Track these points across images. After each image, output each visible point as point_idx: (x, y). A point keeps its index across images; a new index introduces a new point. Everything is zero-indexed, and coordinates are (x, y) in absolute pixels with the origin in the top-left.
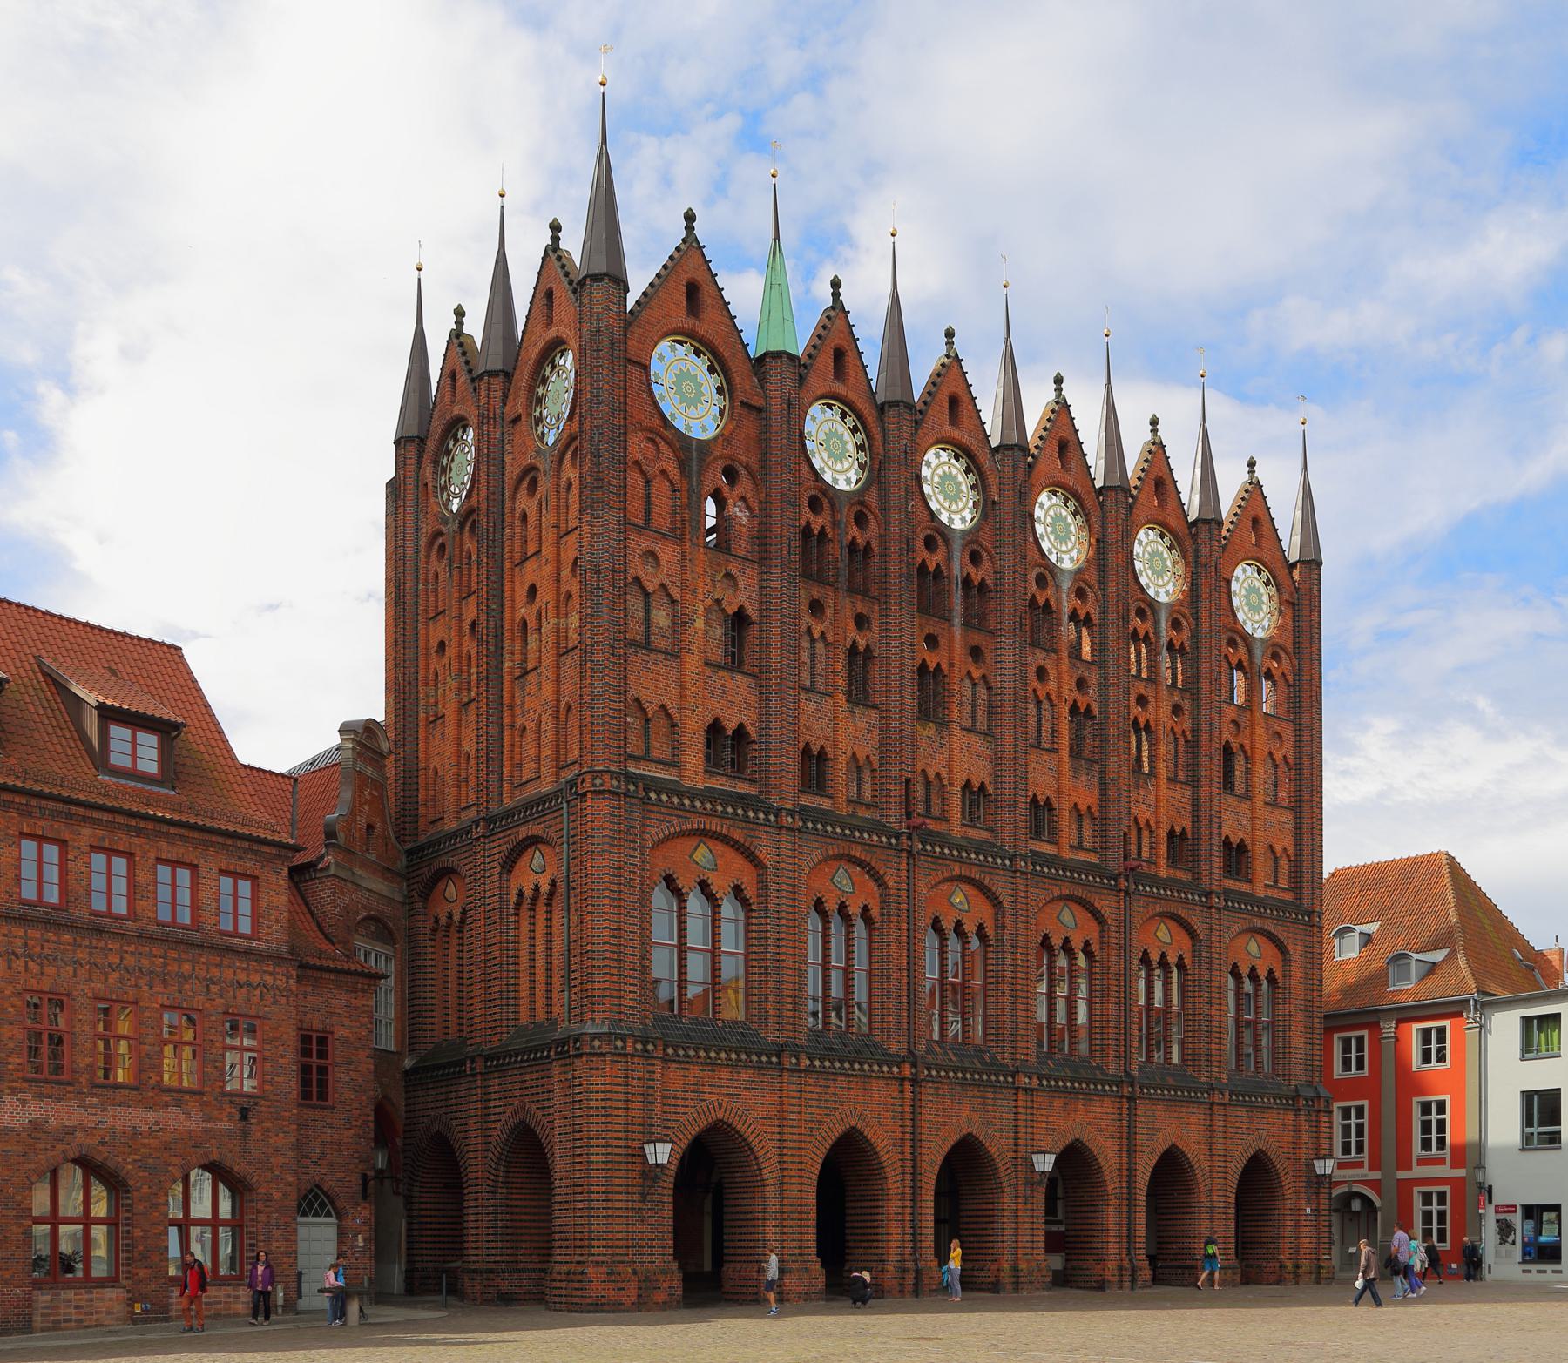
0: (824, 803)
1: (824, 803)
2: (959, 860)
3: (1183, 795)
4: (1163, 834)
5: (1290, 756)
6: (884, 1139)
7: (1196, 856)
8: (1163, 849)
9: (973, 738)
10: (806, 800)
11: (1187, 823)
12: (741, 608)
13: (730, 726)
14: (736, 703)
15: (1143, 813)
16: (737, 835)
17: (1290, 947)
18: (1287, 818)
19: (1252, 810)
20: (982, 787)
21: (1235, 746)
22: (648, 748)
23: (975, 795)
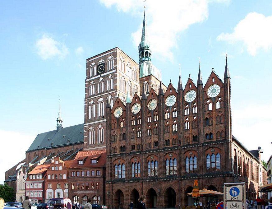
0: (134, 151)
1: (134, 151)
2: (151, 153)
3: (196, 130)
4: (191, 138)
5: (224, 114)
6: (139, 190)
7: (159, 144)
8: (191, 140)
9: (155, 136)
10: (132, 151)
11: (197, 134)
12: (124, 133)
13: (123, 146)
14: (123, 144)
15: (187, 136)
16: (121, 158)
17: (221, 148)
18: (223, 125)
19: (213, 127)
20: (157, 141)
21: (208, 118)
22: (114, 151)
23: (156, 143)
